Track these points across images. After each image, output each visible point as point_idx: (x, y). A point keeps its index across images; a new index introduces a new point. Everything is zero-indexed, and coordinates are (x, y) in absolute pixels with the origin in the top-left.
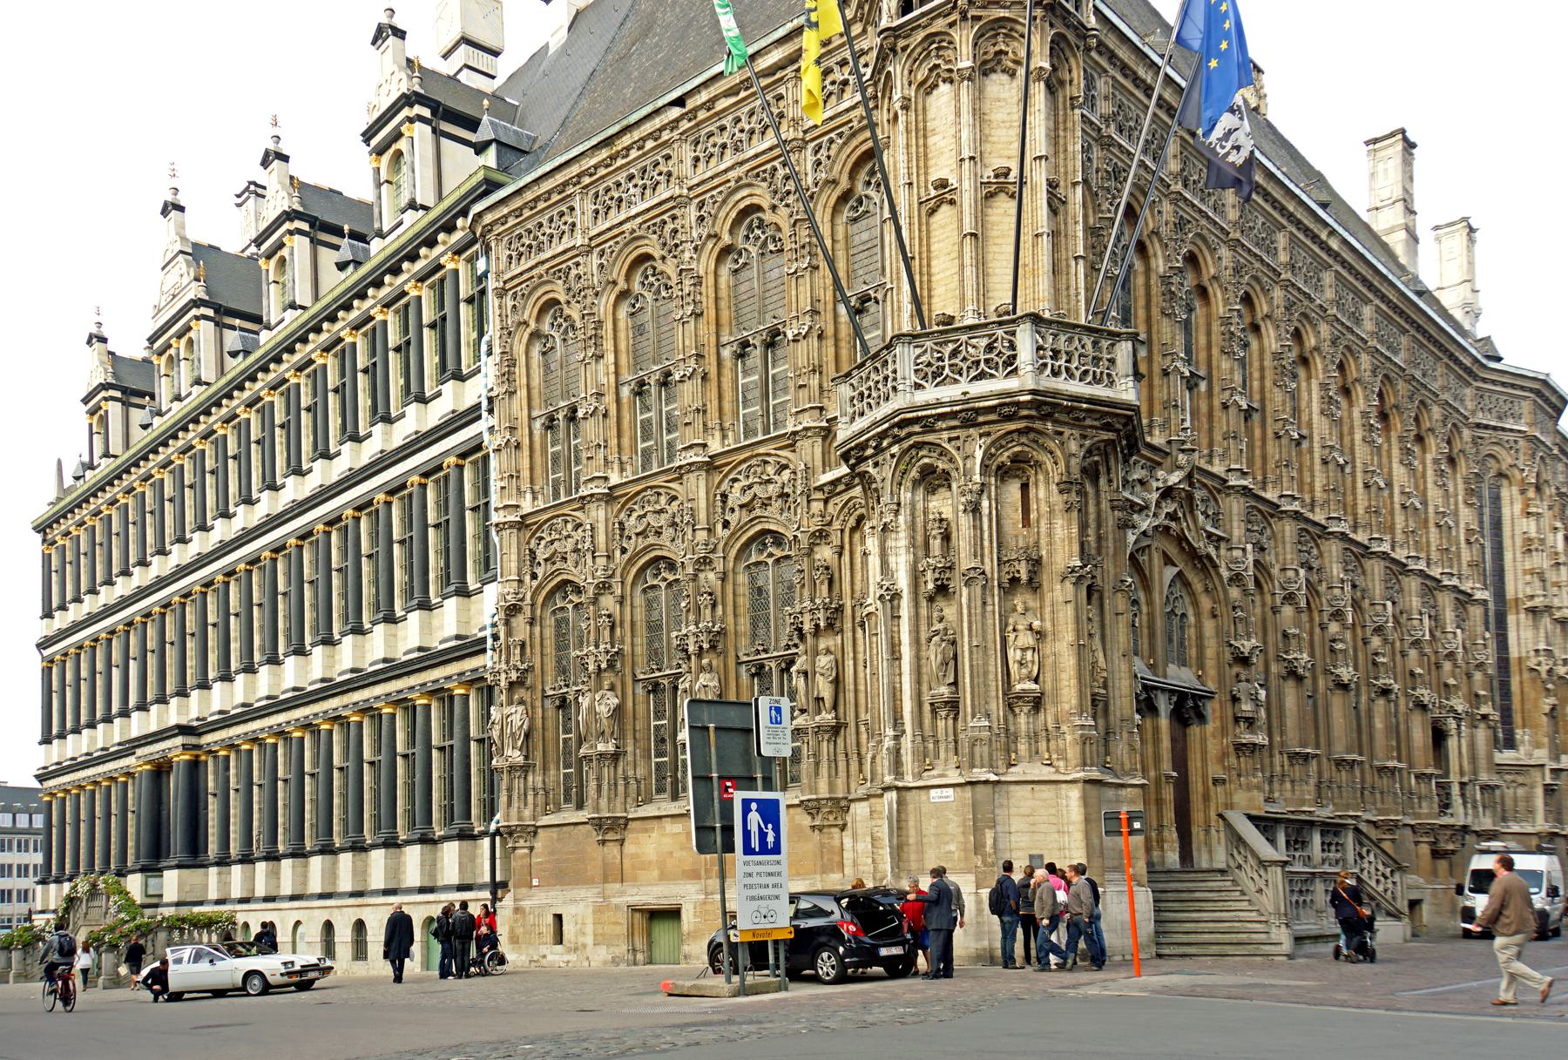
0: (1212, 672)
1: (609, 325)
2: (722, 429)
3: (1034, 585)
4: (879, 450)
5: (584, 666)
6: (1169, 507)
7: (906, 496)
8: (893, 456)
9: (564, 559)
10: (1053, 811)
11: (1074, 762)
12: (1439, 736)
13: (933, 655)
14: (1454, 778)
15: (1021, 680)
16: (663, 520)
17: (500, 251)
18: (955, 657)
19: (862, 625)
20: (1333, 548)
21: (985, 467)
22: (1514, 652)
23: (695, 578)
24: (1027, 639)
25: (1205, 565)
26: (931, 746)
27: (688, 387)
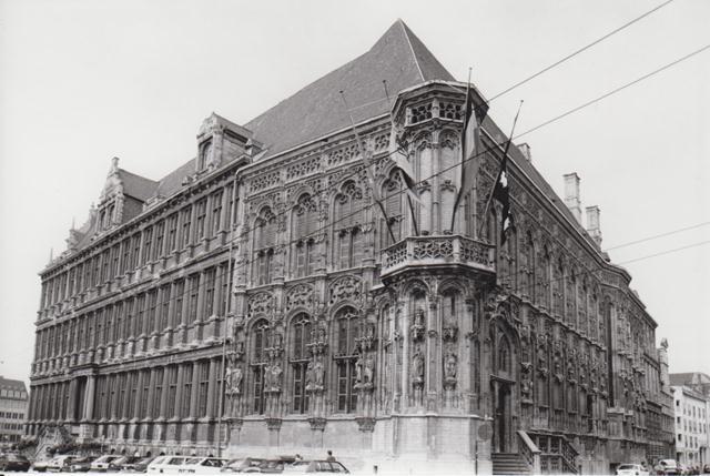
0: (514, 374)
1: (289, 218)
2: (333, 264)
3: (455, 340)
4: (398, 280)
5: (268, 355)
6: (502, 309)
7: (406, 299)
9: (263, 309)
12: (589, 401)
13: (415, 363)
14: (594, 418)
16: (305, 298)
17: (248, 186)
18: (423, 365)
19: (386, 348)
20: (557, 329)
21: (439, 290)
22: (614, 371)
23: (317, 323)
25: (514, 332)
27: (320, 246)
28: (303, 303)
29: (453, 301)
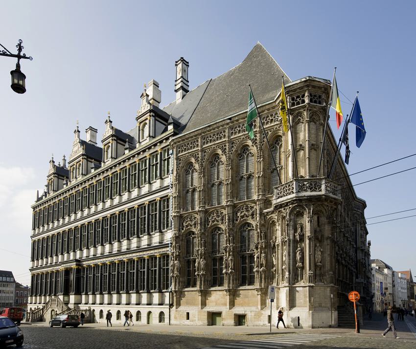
8: (290, 208)
15: (318, 263)
28: (218, 221)
29: (318, 218)
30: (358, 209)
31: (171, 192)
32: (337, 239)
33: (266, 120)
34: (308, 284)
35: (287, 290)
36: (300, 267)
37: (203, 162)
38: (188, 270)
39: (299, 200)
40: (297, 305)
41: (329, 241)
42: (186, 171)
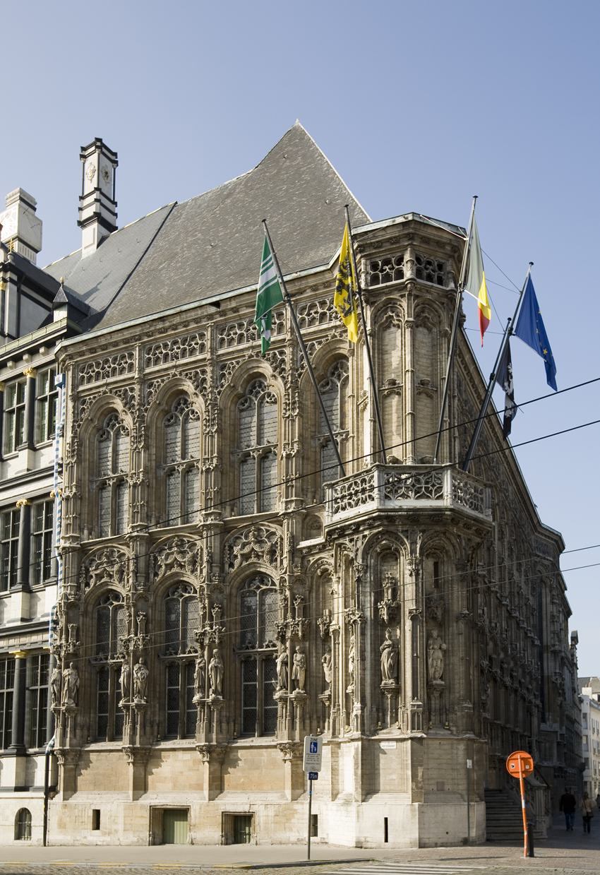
8: (365, 537)
10: (449, 757)
11: (461, 728)
15: (435, 679)
22: (546, 674)
24: (440, 654)
26: (381, 714)
28: (182, 566)
29: (436, 565)
30: (544, 553)
31: (58, 486)
32: (490, 622)
33: (309, 315)
34: (409, 734)
35: (357, 749)
36: (390, 690)
37: (146, 410)
38: (100, 694)
39: (386, 518)
40: (382, 787)
41: (462, 625)
42: (98, 430)
